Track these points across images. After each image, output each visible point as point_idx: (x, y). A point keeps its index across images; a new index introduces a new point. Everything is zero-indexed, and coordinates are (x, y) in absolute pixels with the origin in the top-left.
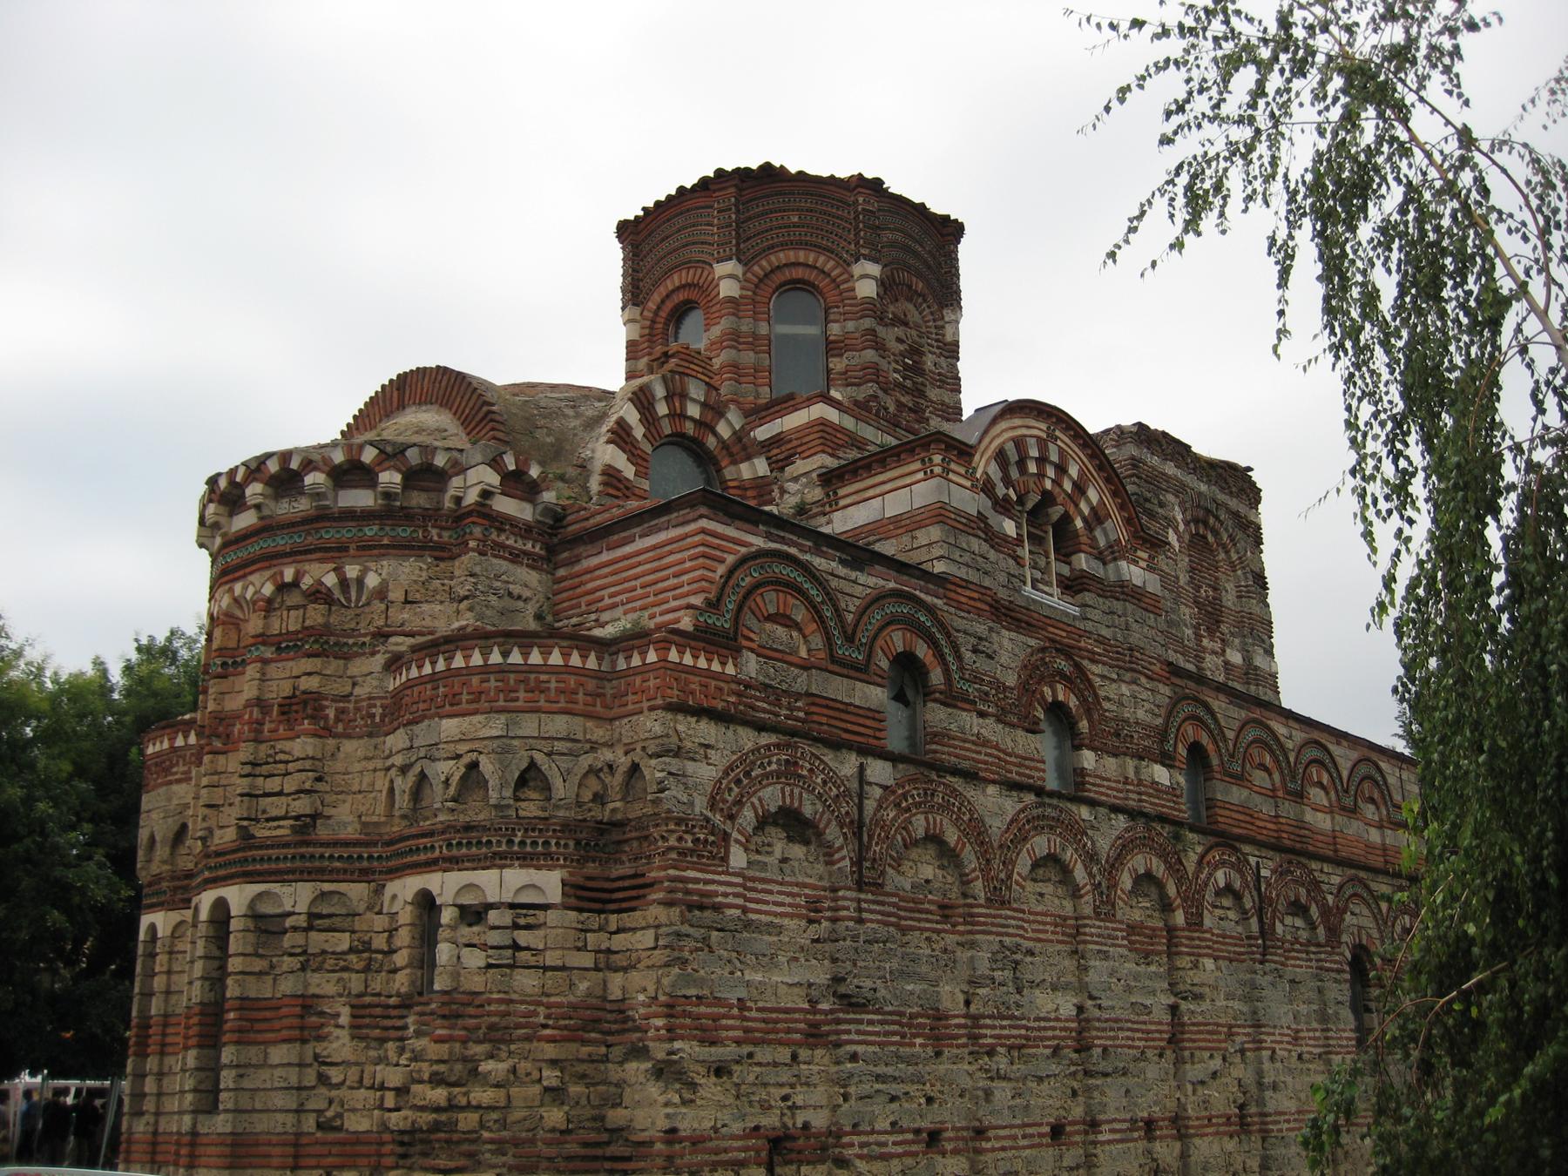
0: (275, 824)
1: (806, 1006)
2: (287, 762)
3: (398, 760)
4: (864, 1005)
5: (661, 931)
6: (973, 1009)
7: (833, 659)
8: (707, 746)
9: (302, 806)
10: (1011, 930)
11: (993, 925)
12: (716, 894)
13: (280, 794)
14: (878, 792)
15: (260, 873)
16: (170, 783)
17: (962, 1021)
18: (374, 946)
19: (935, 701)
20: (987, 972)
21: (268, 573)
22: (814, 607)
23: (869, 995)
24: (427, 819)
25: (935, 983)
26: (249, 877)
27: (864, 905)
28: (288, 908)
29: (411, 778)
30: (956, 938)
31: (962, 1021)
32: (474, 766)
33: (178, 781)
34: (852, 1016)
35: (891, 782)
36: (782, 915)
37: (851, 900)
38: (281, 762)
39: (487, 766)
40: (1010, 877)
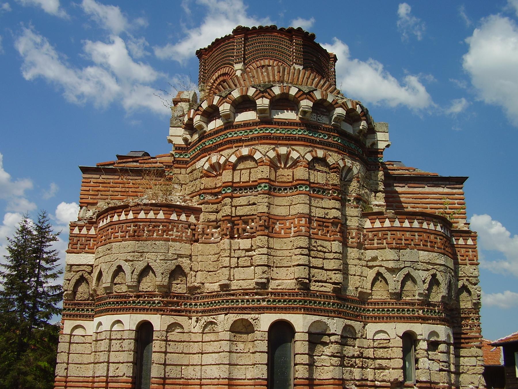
0: (320, 284)
2: (325, 252)
3: (391, 265)
5: (478, 358)
9: (338, 277)
13: (322, 268)
15: (315, 310)
16: (168, 240)
18: (364, 355)
21: (310, 149)
24: (408, 296)
26: (308, 311)
28: (332, 331)
29: (400, 276)
32: (434, 276)
33: (174, 240)
38: (320, 251)
39: (439, 277)
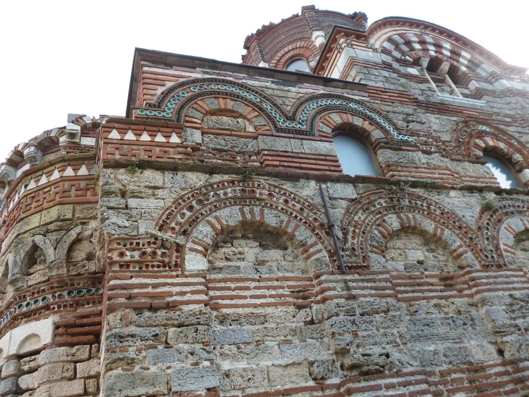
1: (311, 383)
4: (378, 372)
6: (507, 355)
7: (278, 130)
8: (156, 188)
10: (516, 285)
11: (495, 283)
12: (170, 294)
14: (344, 204)
17: (501, 369)
19: (381, 148)
20: (508, 322)
22: (257, 106)
23: (382, 360)
25: (459, 340)
27: (351, 284)
30: (466, 300)
31: (501, 369)
34: (363, 384)
35: (355, 196)
36: (262, 305)
37: (337, 282)
40: (497, 248)
